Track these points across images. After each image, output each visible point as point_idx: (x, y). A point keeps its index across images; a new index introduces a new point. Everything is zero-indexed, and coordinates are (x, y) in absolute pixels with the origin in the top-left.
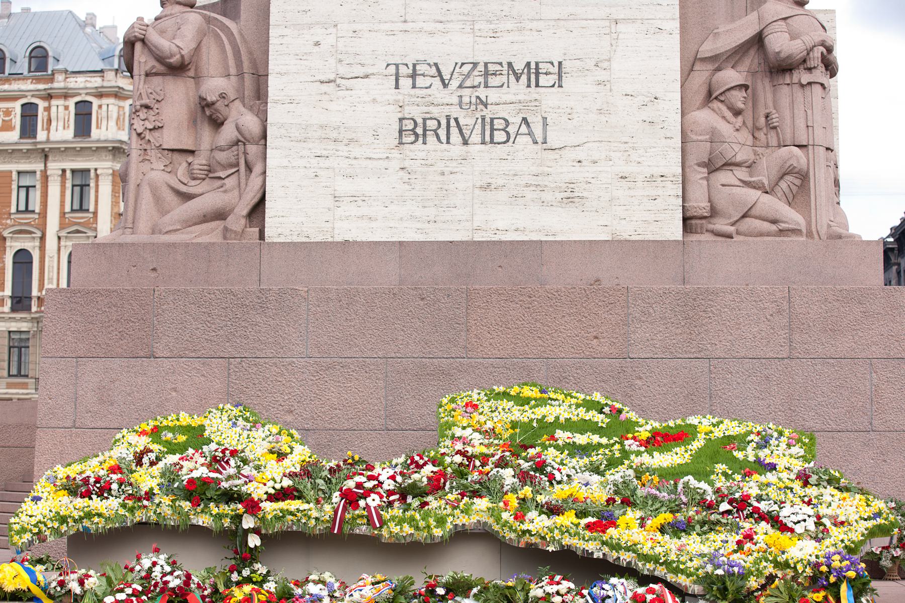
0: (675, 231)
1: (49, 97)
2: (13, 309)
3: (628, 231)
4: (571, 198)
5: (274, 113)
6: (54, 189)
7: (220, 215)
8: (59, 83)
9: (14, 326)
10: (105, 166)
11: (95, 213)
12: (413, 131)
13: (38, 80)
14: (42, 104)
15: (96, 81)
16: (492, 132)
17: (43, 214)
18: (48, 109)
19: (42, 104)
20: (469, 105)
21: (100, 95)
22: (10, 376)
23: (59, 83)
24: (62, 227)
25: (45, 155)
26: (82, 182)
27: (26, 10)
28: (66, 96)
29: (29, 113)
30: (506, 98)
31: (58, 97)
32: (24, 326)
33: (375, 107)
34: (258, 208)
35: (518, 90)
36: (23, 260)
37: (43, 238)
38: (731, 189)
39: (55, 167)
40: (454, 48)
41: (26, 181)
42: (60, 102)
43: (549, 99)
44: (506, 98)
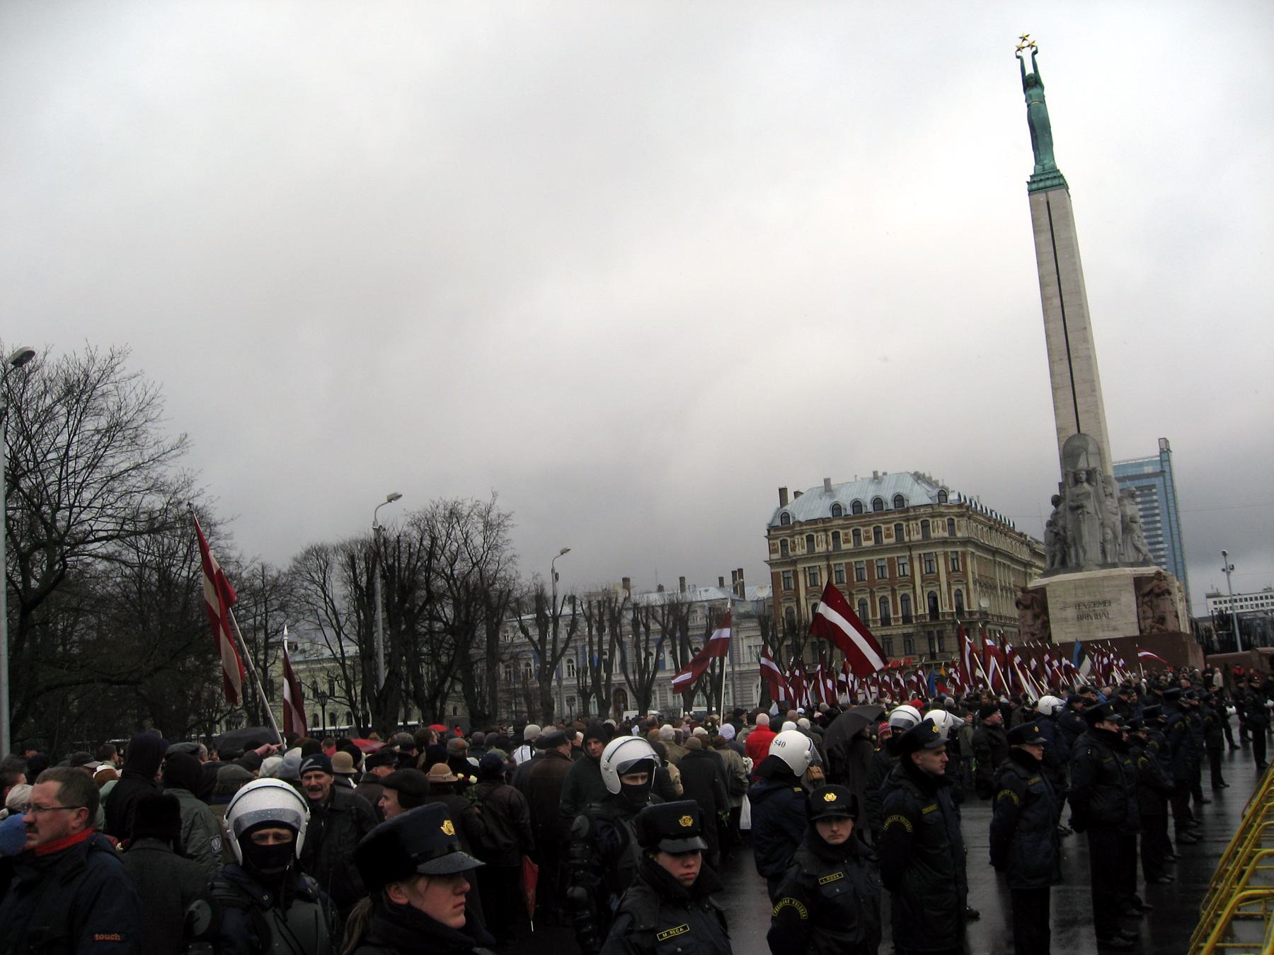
1: (908, 520)
2: (904, 623)
4: (1115, 629)
6: (916, 564)
8: (912, 513)
9: (905, 631)
10: (939, 550)
12: (1080, 618)
13: (901, 512)
14: (905, 524)
15: (929, 510)
20: (1089, 610)
21: (933, 517)
23: (912, 513)
24: (923, 581)
25: (910, 548)
26: (929, 560)
28: (916, 519)
29: (898, 528)
32: (911, 630)
33: (1071, 613)
35: (1101, 607)
36: (905, 599)
37: (914, 588)
39: (915, 553)
41: (902, 561)
43: (1108, 608)
44: (1099, 609)
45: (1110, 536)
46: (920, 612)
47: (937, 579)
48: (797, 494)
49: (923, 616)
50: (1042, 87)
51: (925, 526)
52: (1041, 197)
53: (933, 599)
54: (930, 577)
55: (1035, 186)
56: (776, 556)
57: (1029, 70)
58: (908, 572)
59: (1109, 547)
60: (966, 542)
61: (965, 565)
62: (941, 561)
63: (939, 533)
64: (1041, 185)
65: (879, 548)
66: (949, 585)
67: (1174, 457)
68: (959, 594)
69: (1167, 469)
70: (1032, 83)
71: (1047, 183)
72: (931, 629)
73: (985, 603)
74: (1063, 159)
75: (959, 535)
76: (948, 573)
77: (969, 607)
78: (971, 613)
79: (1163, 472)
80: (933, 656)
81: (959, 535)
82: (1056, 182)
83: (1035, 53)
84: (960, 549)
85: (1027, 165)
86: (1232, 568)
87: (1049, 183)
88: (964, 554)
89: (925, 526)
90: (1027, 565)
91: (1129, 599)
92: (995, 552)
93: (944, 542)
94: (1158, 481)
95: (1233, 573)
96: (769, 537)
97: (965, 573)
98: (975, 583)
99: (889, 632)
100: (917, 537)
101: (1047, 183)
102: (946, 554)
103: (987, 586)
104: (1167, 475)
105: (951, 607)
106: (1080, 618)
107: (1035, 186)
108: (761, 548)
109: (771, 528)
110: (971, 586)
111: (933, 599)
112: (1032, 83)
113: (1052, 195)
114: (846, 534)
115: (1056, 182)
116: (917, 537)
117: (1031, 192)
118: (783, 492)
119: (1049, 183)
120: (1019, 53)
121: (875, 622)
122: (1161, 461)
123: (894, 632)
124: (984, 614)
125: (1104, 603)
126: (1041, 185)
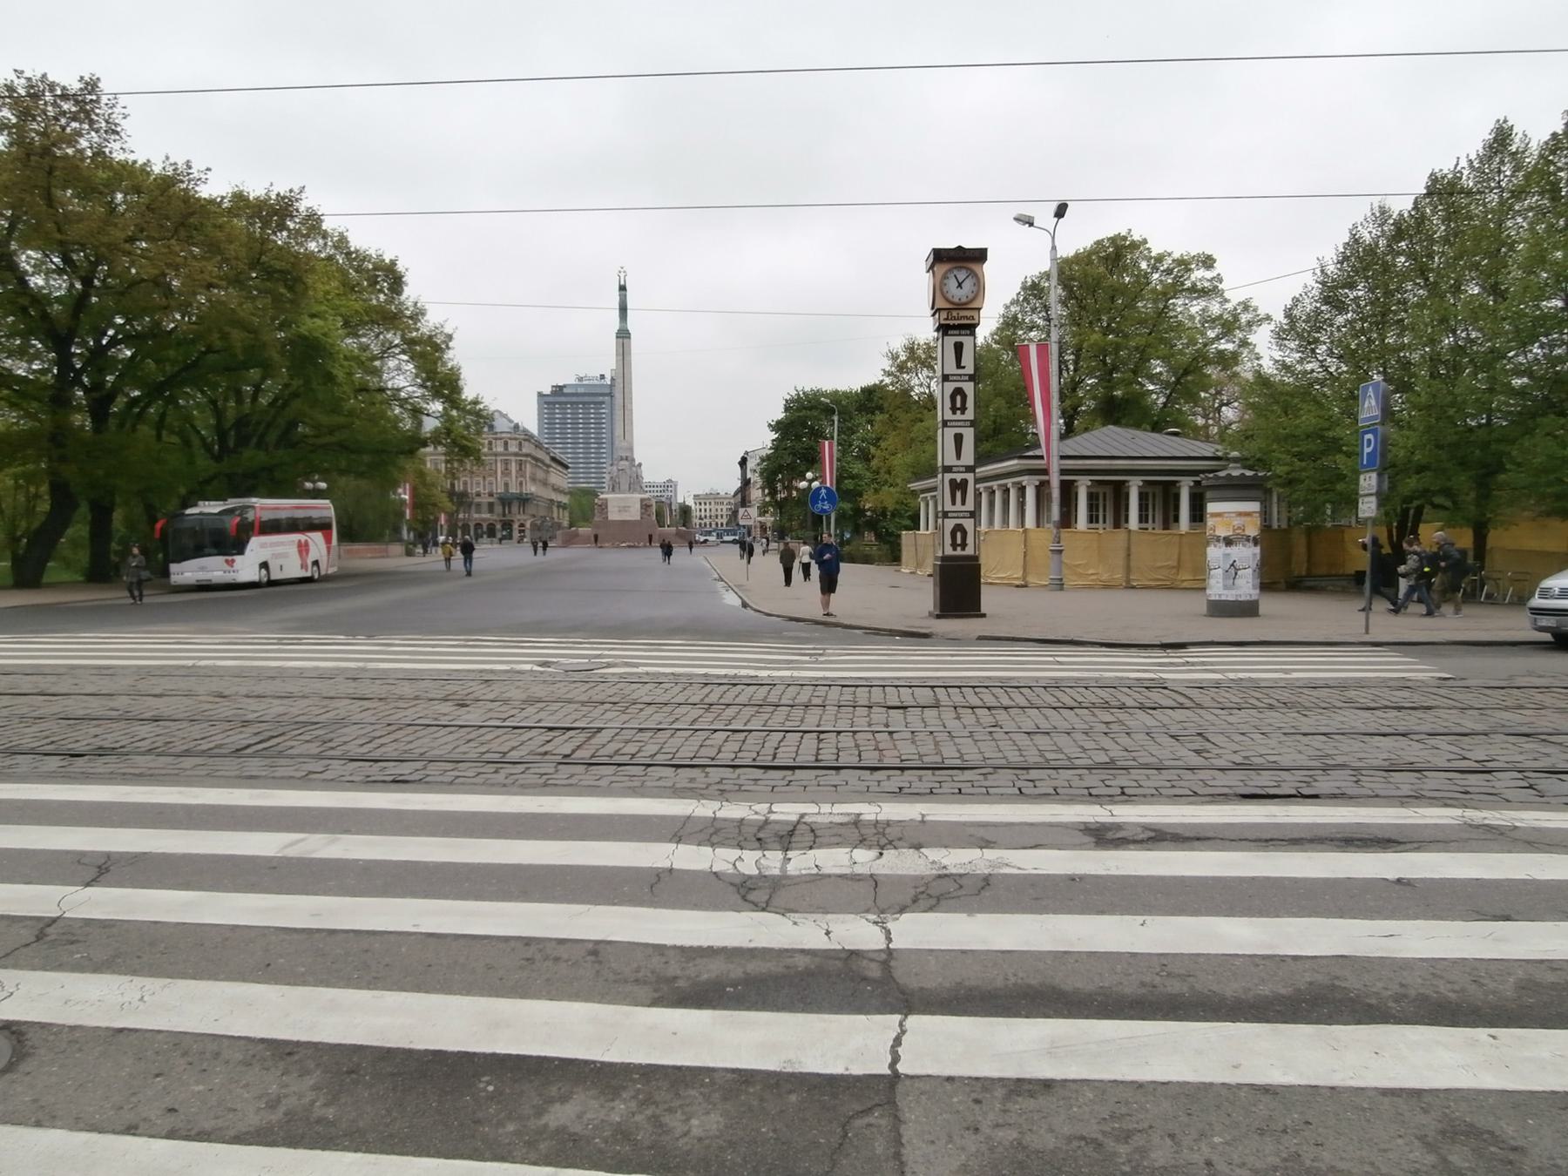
26: (506, 463)
51: (506, 444)
53: (506, 485)
54: (506, 472)
60: (527, 455)
63: (513, 448)
70: (623, 288)
71: (623, 335)
74: (630, 326)
85: (616, 326)
89: (506, 444)
92: (537, 459)
93: (516, 454)
94: (607, 399)
100: (500, 449)
101: (623, 335)
103: (533, 479)
111: (506, 485)
112: (623, 288)
116: (500, 449)
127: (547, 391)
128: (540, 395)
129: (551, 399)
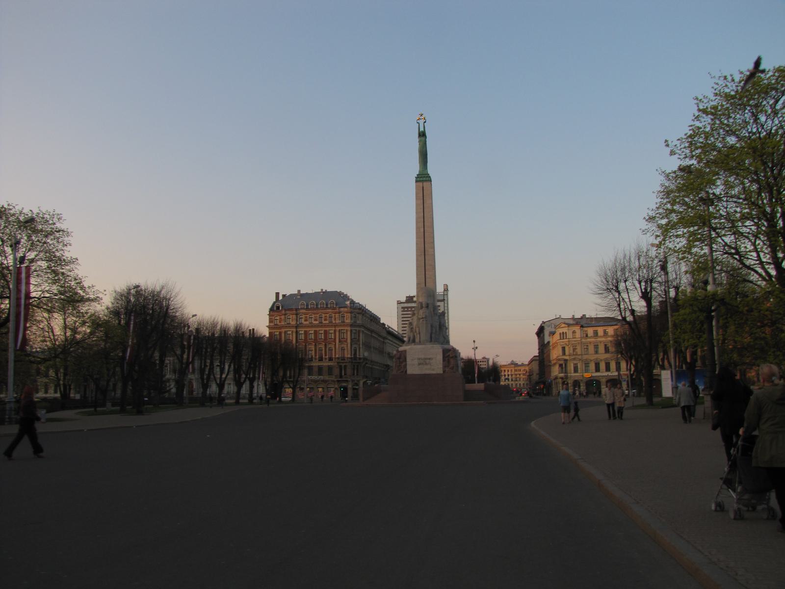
0: (442, 372)
1: (336, 313)
3: (438, 372)
4: (433, 370)
5: (408, 363)
7: (402, 372)
9: (329, 364)
11: (347, 339)
12: (419, 364)
16: (426, 364)
17: (335, 339)
18: (335, 316)
19: (334, 315)
20: (424, 362)
22: (329, 375)
25: (335, 326)
27: (326, 290)
30: (428, 361)
31: (337, 313)
33: (416, 362)
34: (406, 371)
36: (331, 350)
37: (335, 344)
38: (447, 369)
39: (338, 329)
40: (423, 357)
42: (338, 314)
44: (428, 361)
45: (434, 331)
46: (337, 356)
47: (346, 341)
48: (284, 296)
49: (338, 358)
50: (426, 137)
52: (421, 184)
53: (343, 349)
55: (418, 179)
56: (272, 324)
57: (422, 129)
58: (333, 337)
59: (433, 335)
60: (359, 326)
61: (359, 336)
62: (349, 333)
64: (421, 179)
65: (321, 325)
66: (351, 345)
67: (450, 294)
68: (355, 351)
69: (446, 298)
70: (422, 135)
71: (423, 178)
72: (342, 364)
73: (366, 354)
74: (430, 171)
75: (358, 322)
76: (351, 339)
77: (359, 356)
78: (360, 359)
79: (444, 300)
80: (341, 376)
81: (358, 322)
82: (427, 179)
83: (425, 122)
84: (357, 329)
85: (416, 169)
86: (477, 348)
87: (424, 179)
88: (359, 331)
90: (384, 338)
91: (440, 357)
92: (372, 331)
95: (476, 350)
96: (270, 315)
97: (359, 340)
98: (363, 345)
99: (322, 364)
101: (423, 178)
102: (351, 331)
103: (367, 346)
104: (446, 302)
105: (351, 355)
106: (419, 364)
107: (418, 179)
108: (266, 321)
109: (271, 310)
110: (361, 346)
111: (343, 349)
112: (422, 135)
113: (425, 184)
114: (306, 317)
115: (427, 179)
117: (416, 181)
118: (277, 294)
119: (424, 179)
120: (418, 121)
121: (316, 359)
122: (444, 295)
123: (324, 364)
124: (365, 359)
125: (430, 359)
126: (421, 179)
127: (404, 299)
128: (399, 303)
129: (406, 305)
